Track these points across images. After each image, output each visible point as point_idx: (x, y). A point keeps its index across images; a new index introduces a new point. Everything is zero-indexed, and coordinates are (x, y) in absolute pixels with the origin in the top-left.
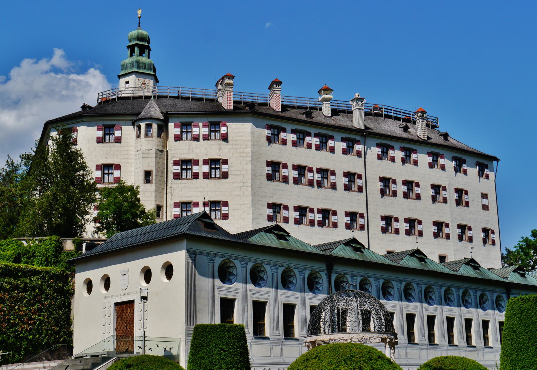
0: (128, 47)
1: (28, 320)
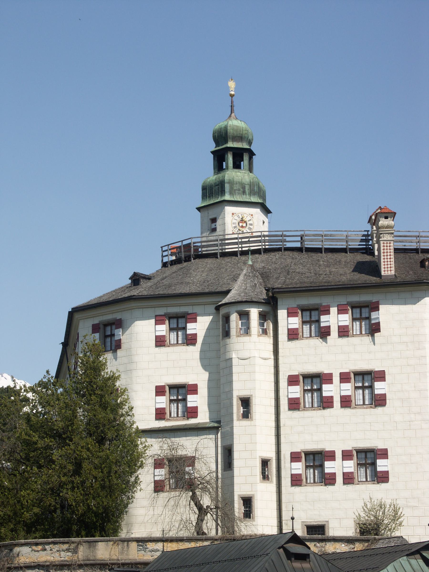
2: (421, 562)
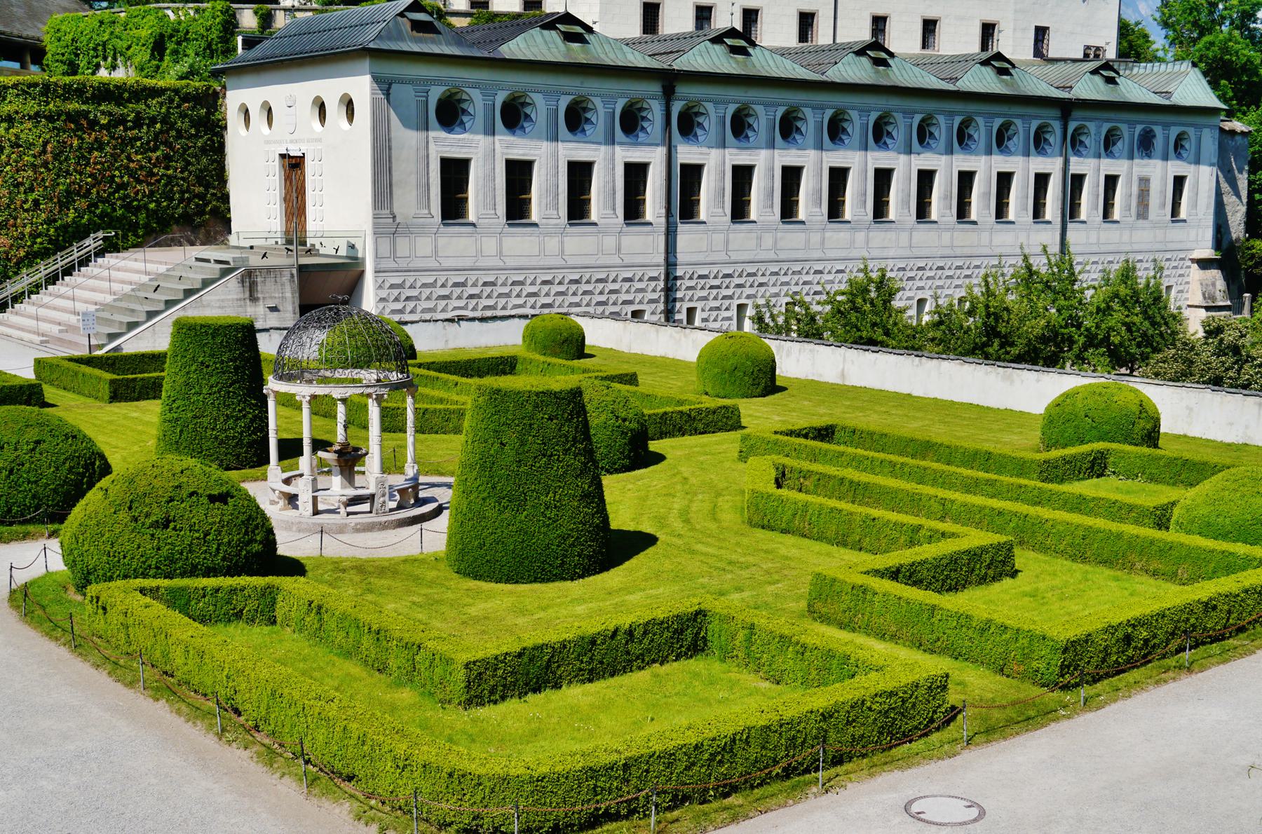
1: (147, 176)
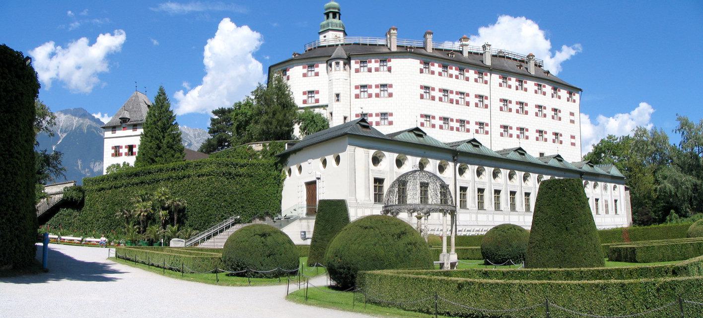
0: (326, 14)
2: (413, 134)
